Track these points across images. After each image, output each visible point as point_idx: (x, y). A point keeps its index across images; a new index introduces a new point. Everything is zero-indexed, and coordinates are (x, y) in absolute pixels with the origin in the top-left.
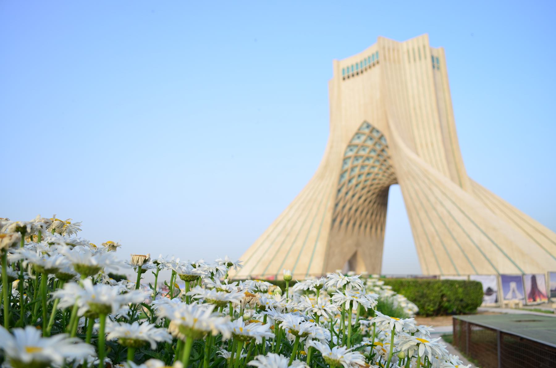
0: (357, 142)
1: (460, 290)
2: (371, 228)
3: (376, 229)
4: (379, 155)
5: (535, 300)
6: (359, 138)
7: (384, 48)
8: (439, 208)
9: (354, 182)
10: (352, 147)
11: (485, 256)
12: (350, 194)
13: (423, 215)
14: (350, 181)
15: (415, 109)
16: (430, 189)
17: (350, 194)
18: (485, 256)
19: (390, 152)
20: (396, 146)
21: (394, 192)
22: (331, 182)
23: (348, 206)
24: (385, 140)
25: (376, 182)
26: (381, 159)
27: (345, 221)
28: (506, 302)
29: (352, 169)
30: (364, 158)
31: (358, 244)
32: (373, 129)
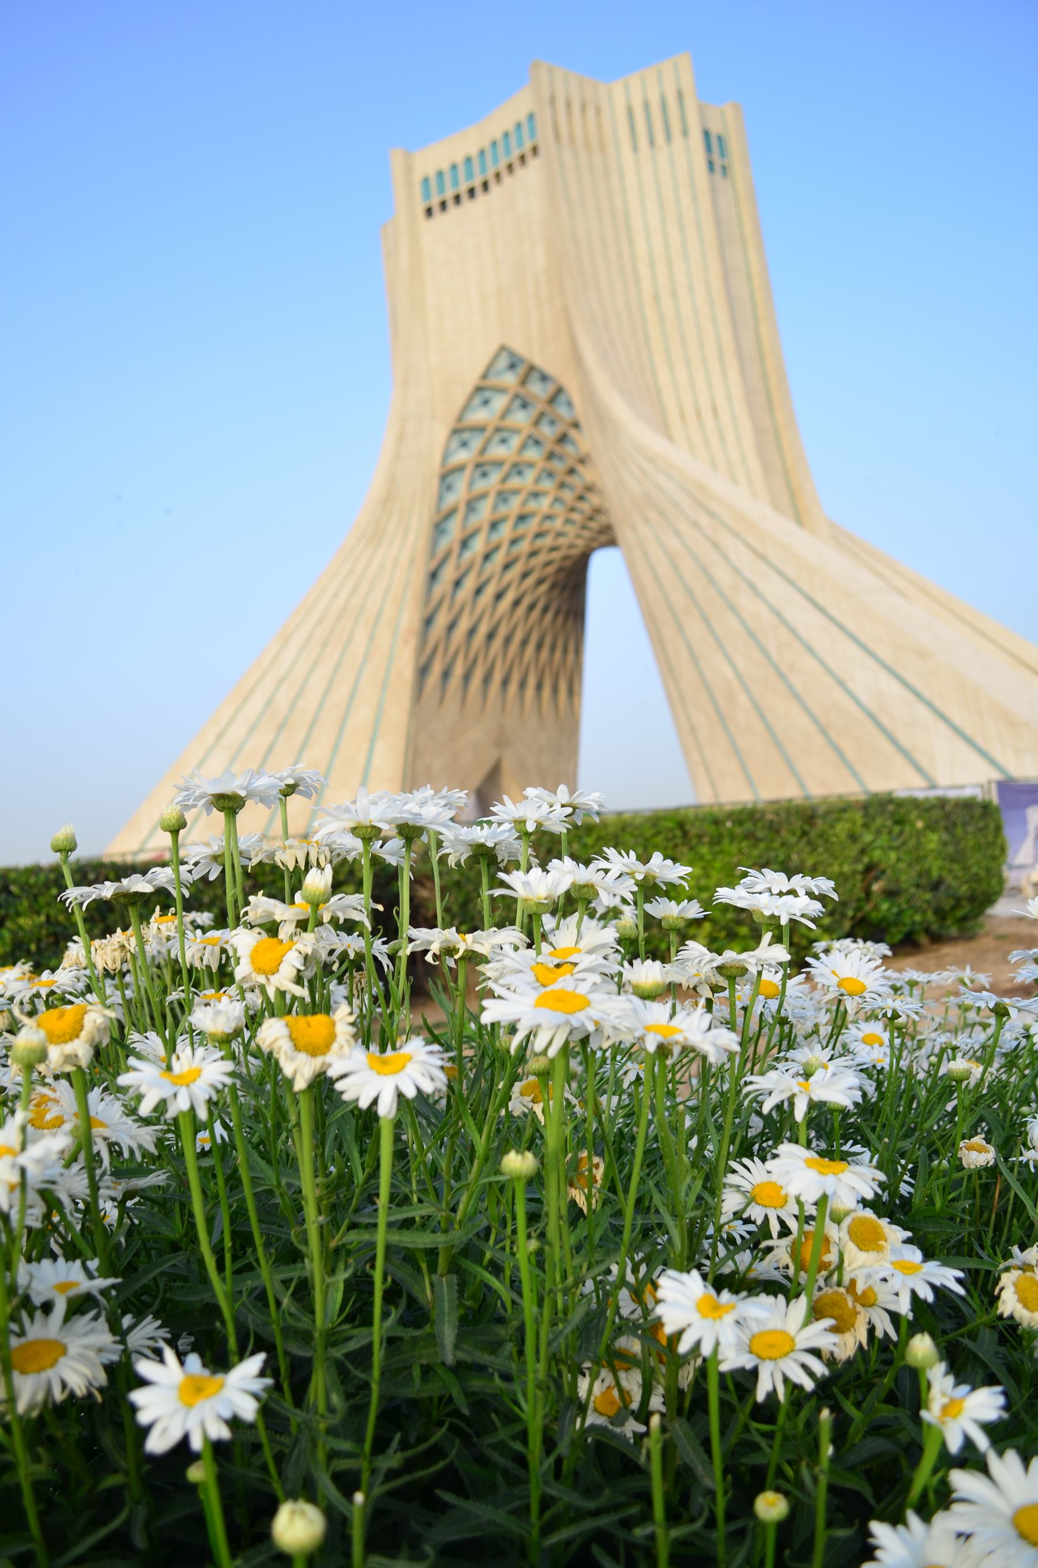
0: (479, 416)
1: (933, 841)
2: (539, 687)
3: (555, 690)
4: (551, 456)
6: (486, 402)
7: (553, 100)
8: (746, 602)
9: (478, 546)
10: (466, 436)
11: (893, 741)
12: (470, 584)
13: (695, 628)
15: (657, 299)
16: (716, 545)
17: (470, 584)
18: (893, 741)
19: (585, 442)
20: (603, 418)
21: (605, 571)
22: (406, 550)
23: (464, 625)
24: (569, 404)
25: (547, 541)
26: (559, 466)
27: (459, 670)
29: (471, 506)
30: (506, 468)
31: (501, 741)
32: (531, 372)
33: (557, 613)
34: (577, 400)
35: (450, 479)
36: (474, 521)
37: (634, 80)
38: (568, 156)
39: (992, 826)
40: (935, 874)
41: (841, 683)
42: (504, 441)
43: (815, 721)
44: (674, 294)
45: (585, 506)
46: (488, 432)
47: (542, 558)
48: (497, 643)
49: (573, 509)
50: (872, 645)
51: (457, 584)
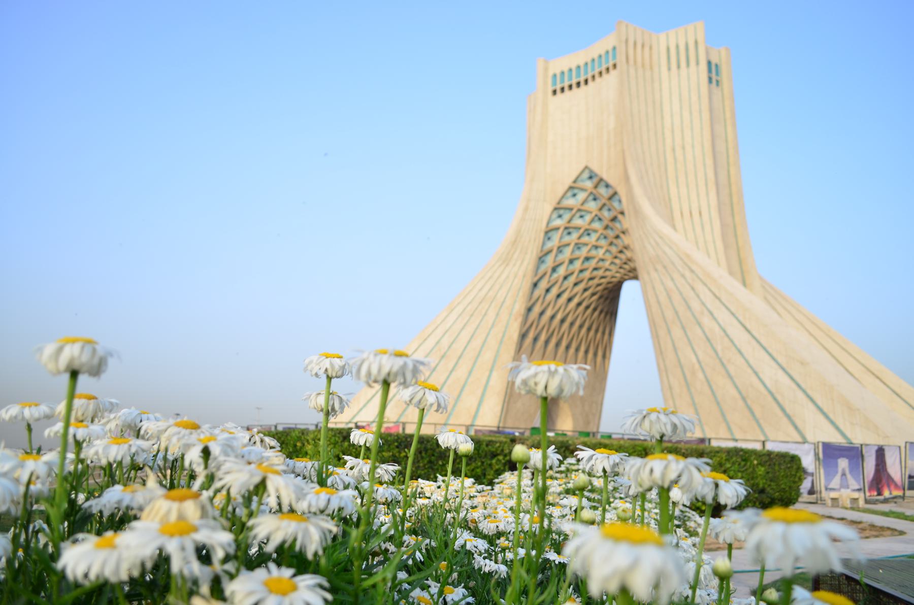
0: (570, 202)
1: (761, 470)
2: (586, 352)
3: (595, 354)
5: (879, 494)
6: (574, 195)
7: (627, 41)
8: (706, 321)
9: (562, 271)
10: (561, 212)
11: (783, 410)
12: (554, 291)
13: (677, 332)
14: (554, 270)
15: (674, 150)
16: (693, 289)
17: (554, 291)
18: (783, 410)
19: (626, 222)
20: (637, 211)
21: (630, 292)
23: (549, 313)
24: (620, 201)
25: (600, 273)
26: (610, 233)
27: (543, 337)
28: (833, 495)
29: (560, 250)
30: (581, 231)
33: (601, 312)
34: (624, 200)
35: (550, 234)
36: (561, 257)
37: (672, 33)
38: (632, 71)
39: (795, 467)
40: (761, 486)
41: (756, 373)
42: (581, 217)
43: (740, 393)
44: (683, 148)
45: (623, 256)
46: (574, 211)
47: (596, 281)
48: (566, 325)
49: (616, 257)
50: (775, 355)
51: (548, 291)
